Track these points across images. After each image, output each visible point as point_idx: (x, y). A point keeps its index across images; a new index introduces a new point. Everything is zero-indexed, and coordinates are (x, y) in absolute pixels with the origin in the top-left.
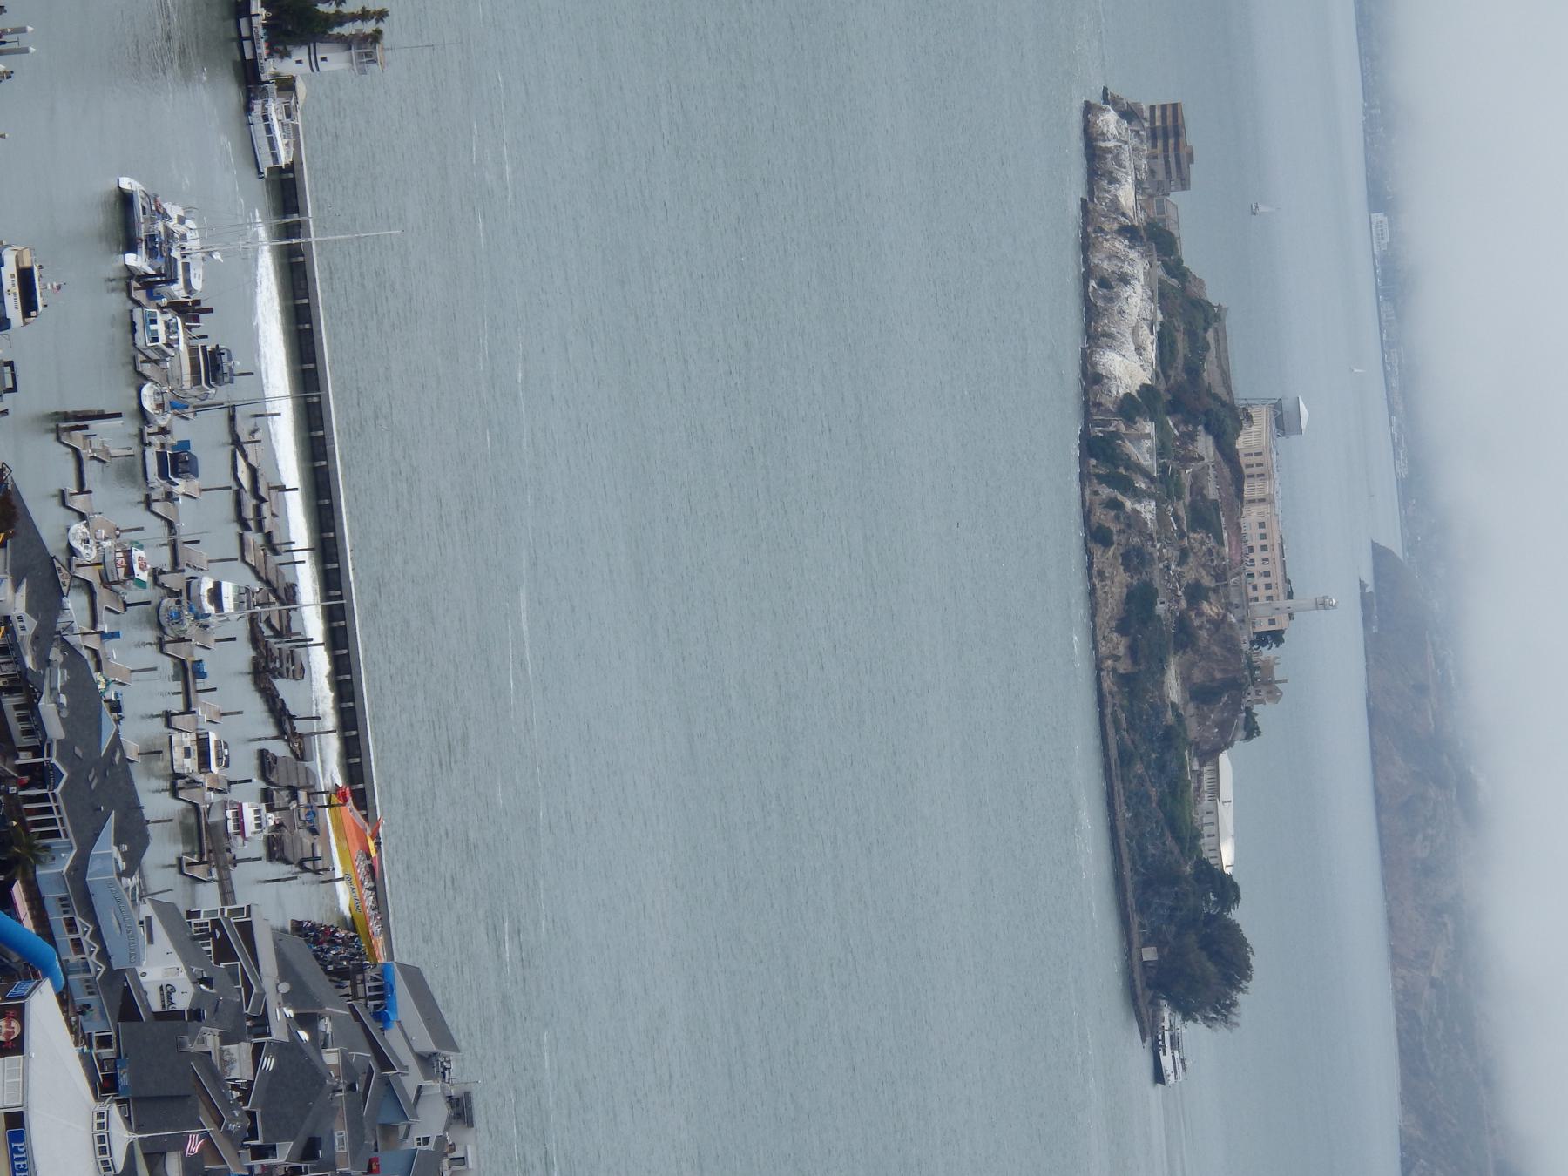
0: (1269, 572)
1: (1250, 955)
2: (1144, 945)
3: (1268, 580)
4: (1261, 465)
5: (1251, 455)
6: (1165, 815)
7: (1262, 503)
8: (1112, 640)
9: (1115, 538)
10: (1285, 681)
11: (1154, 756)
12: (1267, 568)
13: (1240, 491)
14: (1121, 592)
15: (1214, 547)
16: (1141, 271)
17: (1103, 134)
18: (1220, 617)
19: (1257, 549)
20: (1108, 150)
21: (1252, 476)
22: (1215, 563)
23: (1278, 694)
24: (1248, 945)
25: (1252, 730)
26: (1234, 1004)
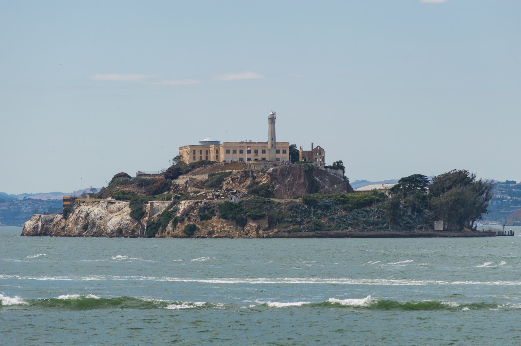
0: (255, 150)
1: (455, 171)
2: (433, 228)
3: (260, 151)
4: (201, 151)
5: (194, 157)
6: (355, 208)
7: (219, 152)
8: (249, 230)
9: (191, 223)
10: (312, 144)
11: (319, 211)
12: (253, 151)
13: (211, 163)
14: (222, 222)
15: (231, 177)
16: (85, 207)
17: (34, 228)
18: (269, 176)
19: (241, 156)
20: (43, 225)
21: (207, 157)
22: (239, 177)
23: (318, 148)
24: (449, 173)
25: (339, 166)
26: (480, 182)
